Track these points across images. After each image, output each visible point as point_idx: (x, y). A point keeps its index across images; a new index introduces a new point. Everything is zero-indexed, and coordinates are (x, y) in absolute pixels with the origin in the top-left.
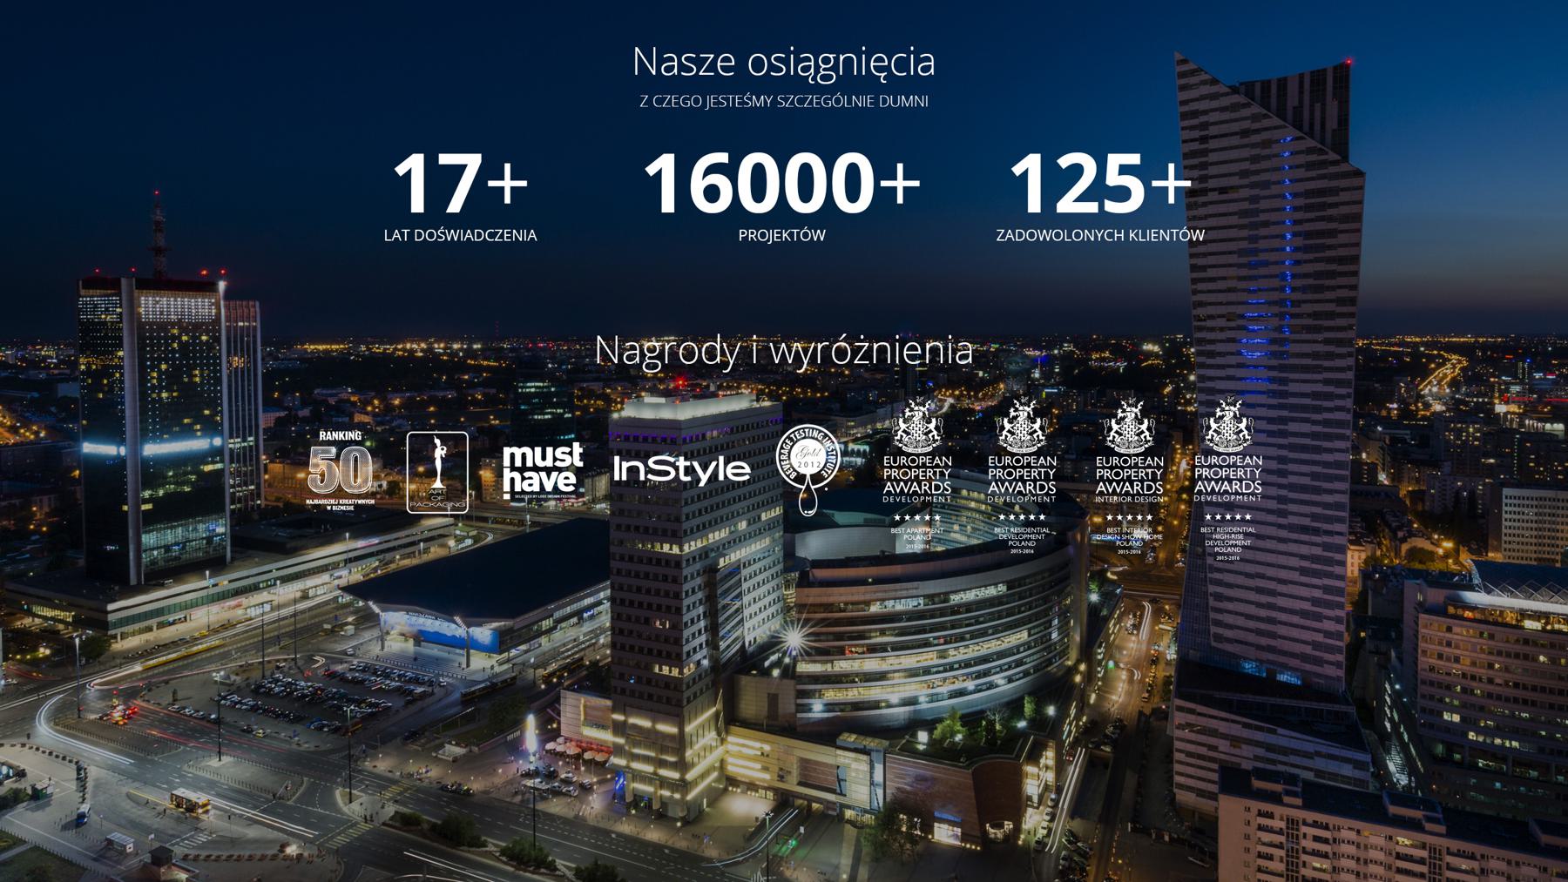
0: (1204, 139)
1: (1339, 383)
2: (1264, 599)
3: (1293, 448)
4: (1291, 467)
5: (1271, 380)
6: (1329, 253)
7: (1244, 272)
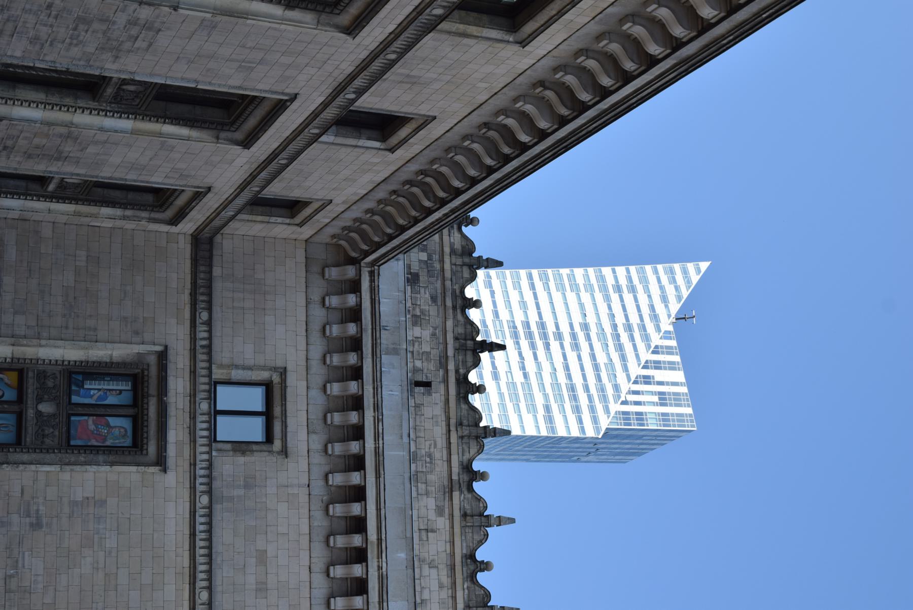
6: (510, 406)
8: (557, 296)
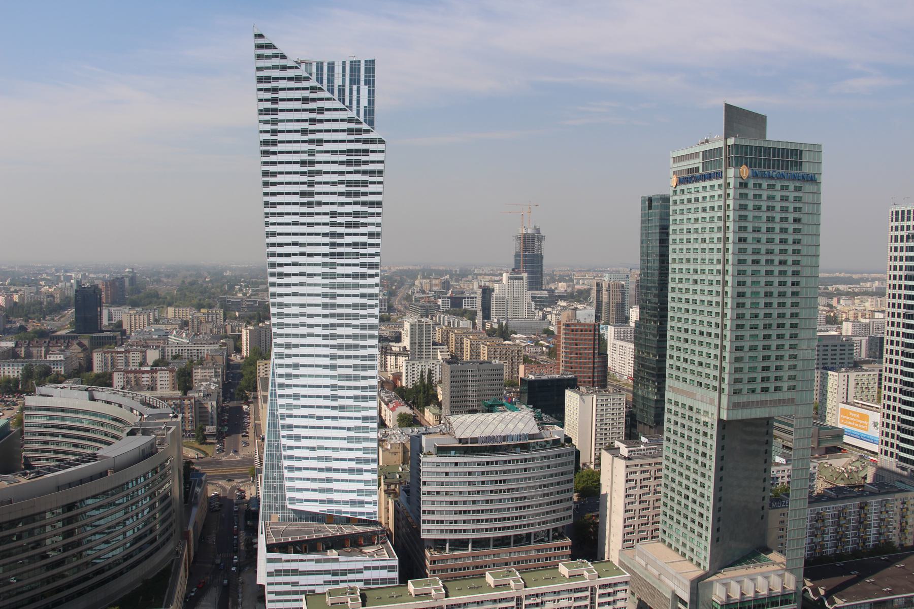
0: (275, 101)
1: (371, 296)
2: (323, 465)
3: (340, 347)
4: (339, 362)
5: (325, 295)
7: (305, 209)
8: (280, 147)
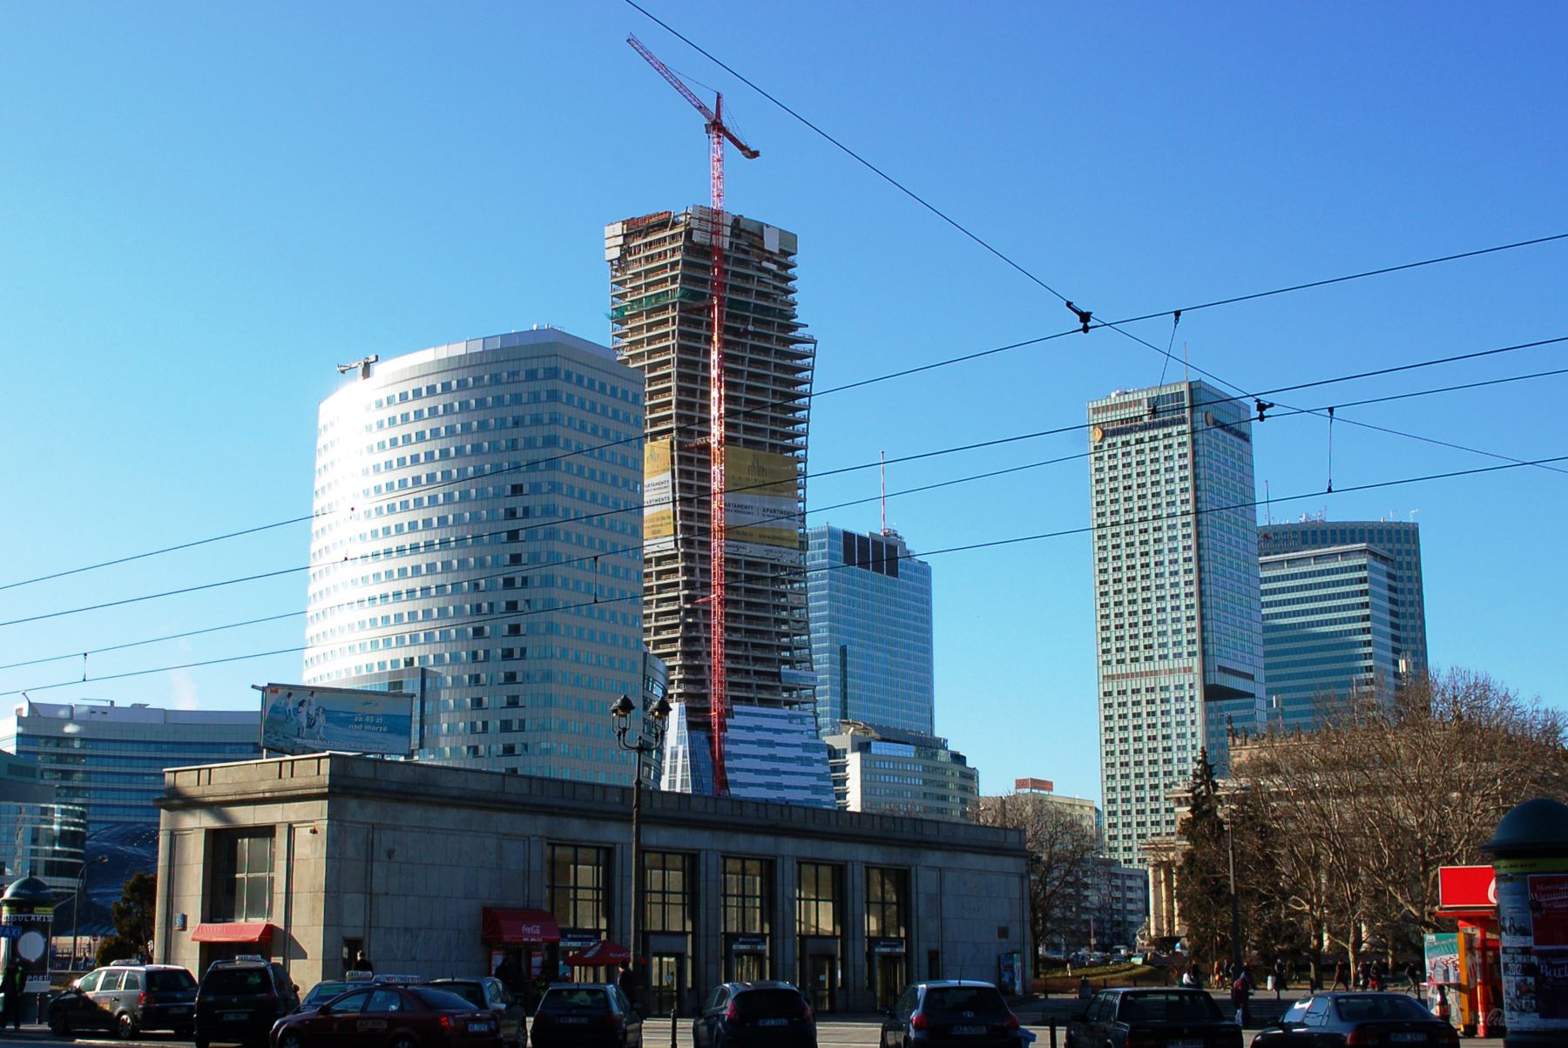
2: (765, 751)
